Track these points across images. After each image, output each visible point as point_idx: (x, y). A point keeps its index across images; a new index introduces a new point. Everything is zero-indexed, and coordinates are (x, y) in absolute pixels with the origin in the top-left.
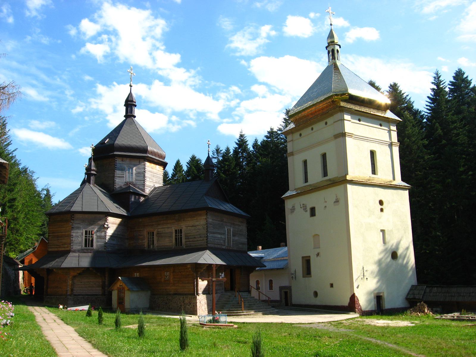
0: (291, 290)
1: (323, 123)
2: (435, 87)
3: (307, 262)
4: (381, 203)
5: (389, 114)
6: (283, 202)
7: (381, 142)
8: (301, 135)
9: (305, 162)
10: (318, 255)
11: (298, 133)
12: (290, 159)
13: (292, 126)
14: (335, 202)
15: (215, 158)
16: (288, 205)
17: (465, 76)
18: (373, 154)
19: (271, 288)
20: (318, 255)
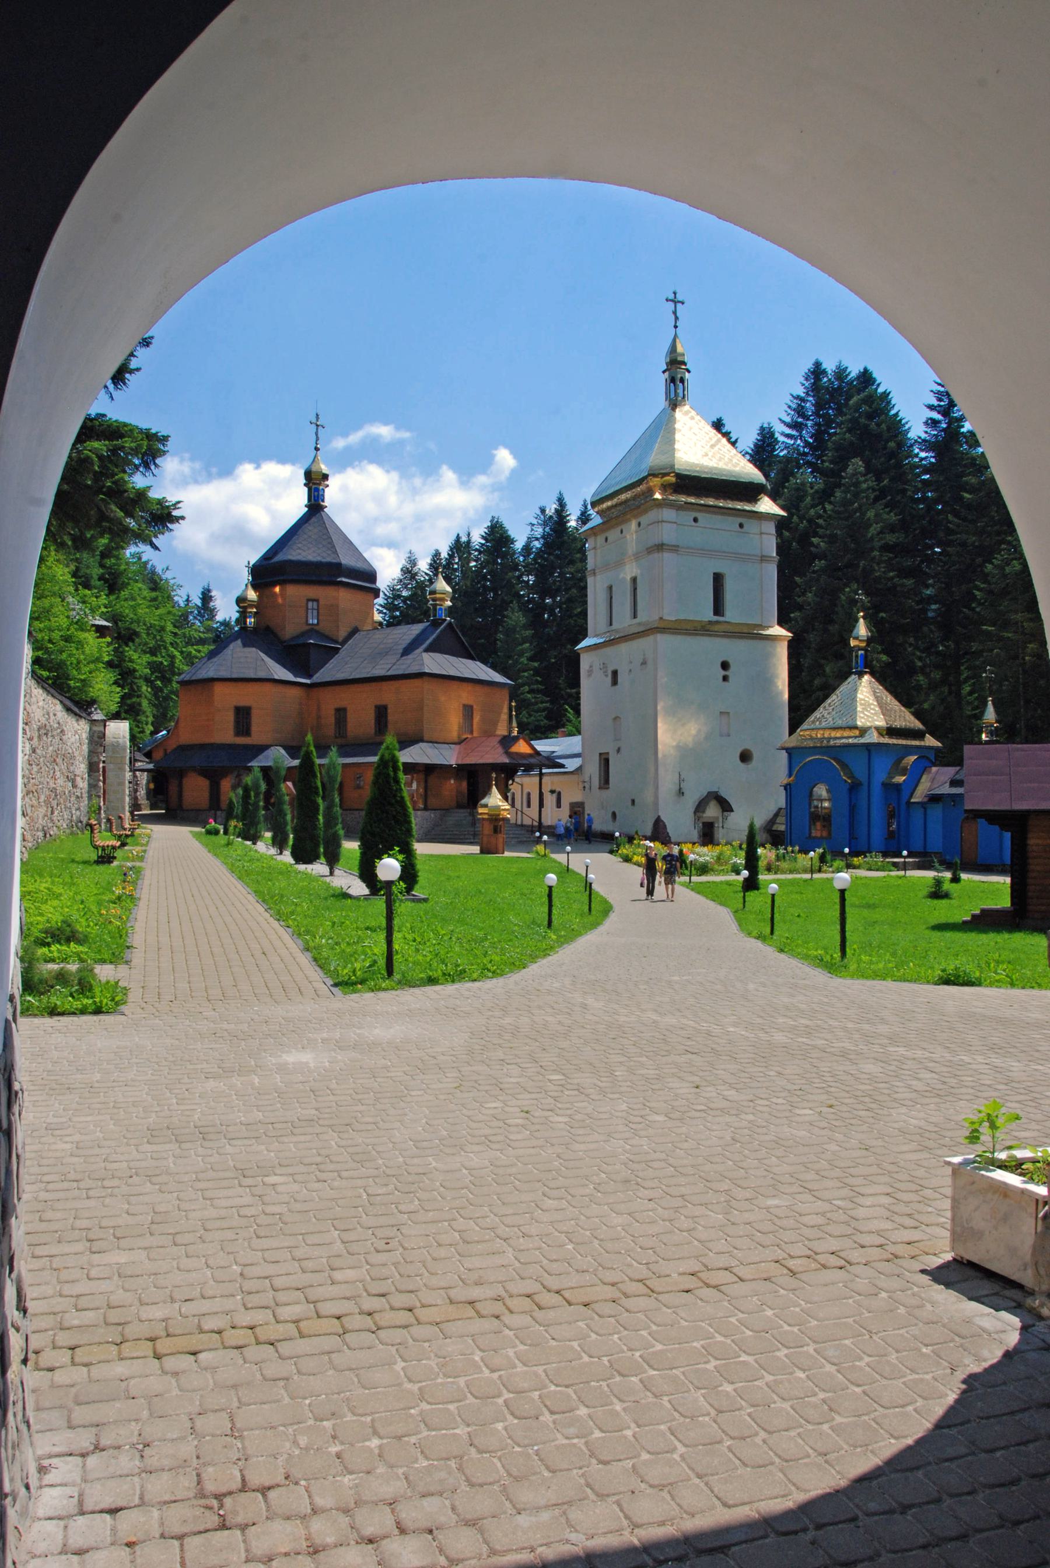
0: (584, 808)
3: (605, 761)
4: (725, 666)
5: (766, 505)
8: (606, 539)
9: (610, 588)
10: (619, 750)
11: (603, 536)
12: (590, 580)
14: (642, 664)
15: (537, 539)
16: (585, 662)
18: (718, 580)
19: (559, 805)
20: (619, 750)
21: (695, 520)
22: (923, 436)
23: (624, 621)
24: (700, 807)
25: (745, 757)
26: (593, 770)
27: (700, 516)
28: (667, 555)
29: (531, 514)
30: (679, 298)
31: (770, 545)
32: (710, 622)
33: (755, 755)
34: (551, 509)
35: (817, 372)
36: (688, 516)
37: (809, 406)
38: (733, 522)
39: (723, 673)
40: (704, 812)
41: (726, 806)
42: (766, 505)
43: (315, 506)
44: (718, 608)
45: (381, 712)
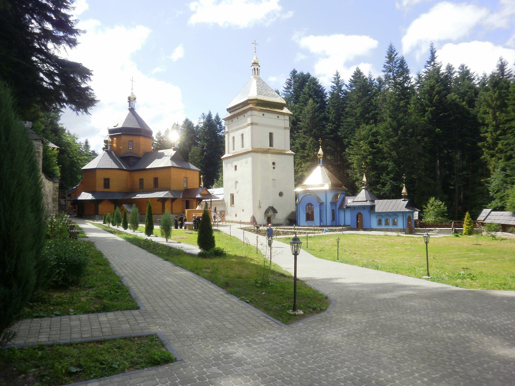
1: (243, 116)
2: (335, 85)
3: (232, 196)
5: (286, 110)
6: (221, 160)
7: (278, 127)
9: (234, 138)
10: (237, 193)
13: (229, 115)
17: (352, 79)
18: (271, 135)
21: (263, 115)
22: (331, 91)
23: (239, 149)
24: (267, 212)
25: (281, 194)
26: (228, 200)
27: (264, 113)
28: (254, 126)
29: (200, 115)
30: (256, 43)
31: (287, 124)
32: (269, 149)
33: (284, 194)
34: (207, 114)
35: (294, 72)
36: (261, 114)
37: (292, 82)
38: (275, 116)
39: (273, 166)
40: (268, 213)
41: (275, 211)
42: (286, 110)
43: (132, 110)
44: (271, 145)
45: (156, 180)
